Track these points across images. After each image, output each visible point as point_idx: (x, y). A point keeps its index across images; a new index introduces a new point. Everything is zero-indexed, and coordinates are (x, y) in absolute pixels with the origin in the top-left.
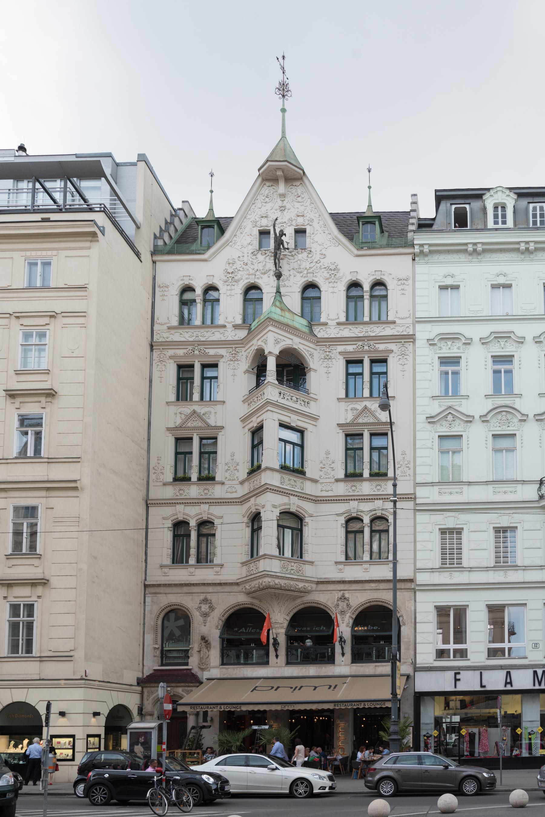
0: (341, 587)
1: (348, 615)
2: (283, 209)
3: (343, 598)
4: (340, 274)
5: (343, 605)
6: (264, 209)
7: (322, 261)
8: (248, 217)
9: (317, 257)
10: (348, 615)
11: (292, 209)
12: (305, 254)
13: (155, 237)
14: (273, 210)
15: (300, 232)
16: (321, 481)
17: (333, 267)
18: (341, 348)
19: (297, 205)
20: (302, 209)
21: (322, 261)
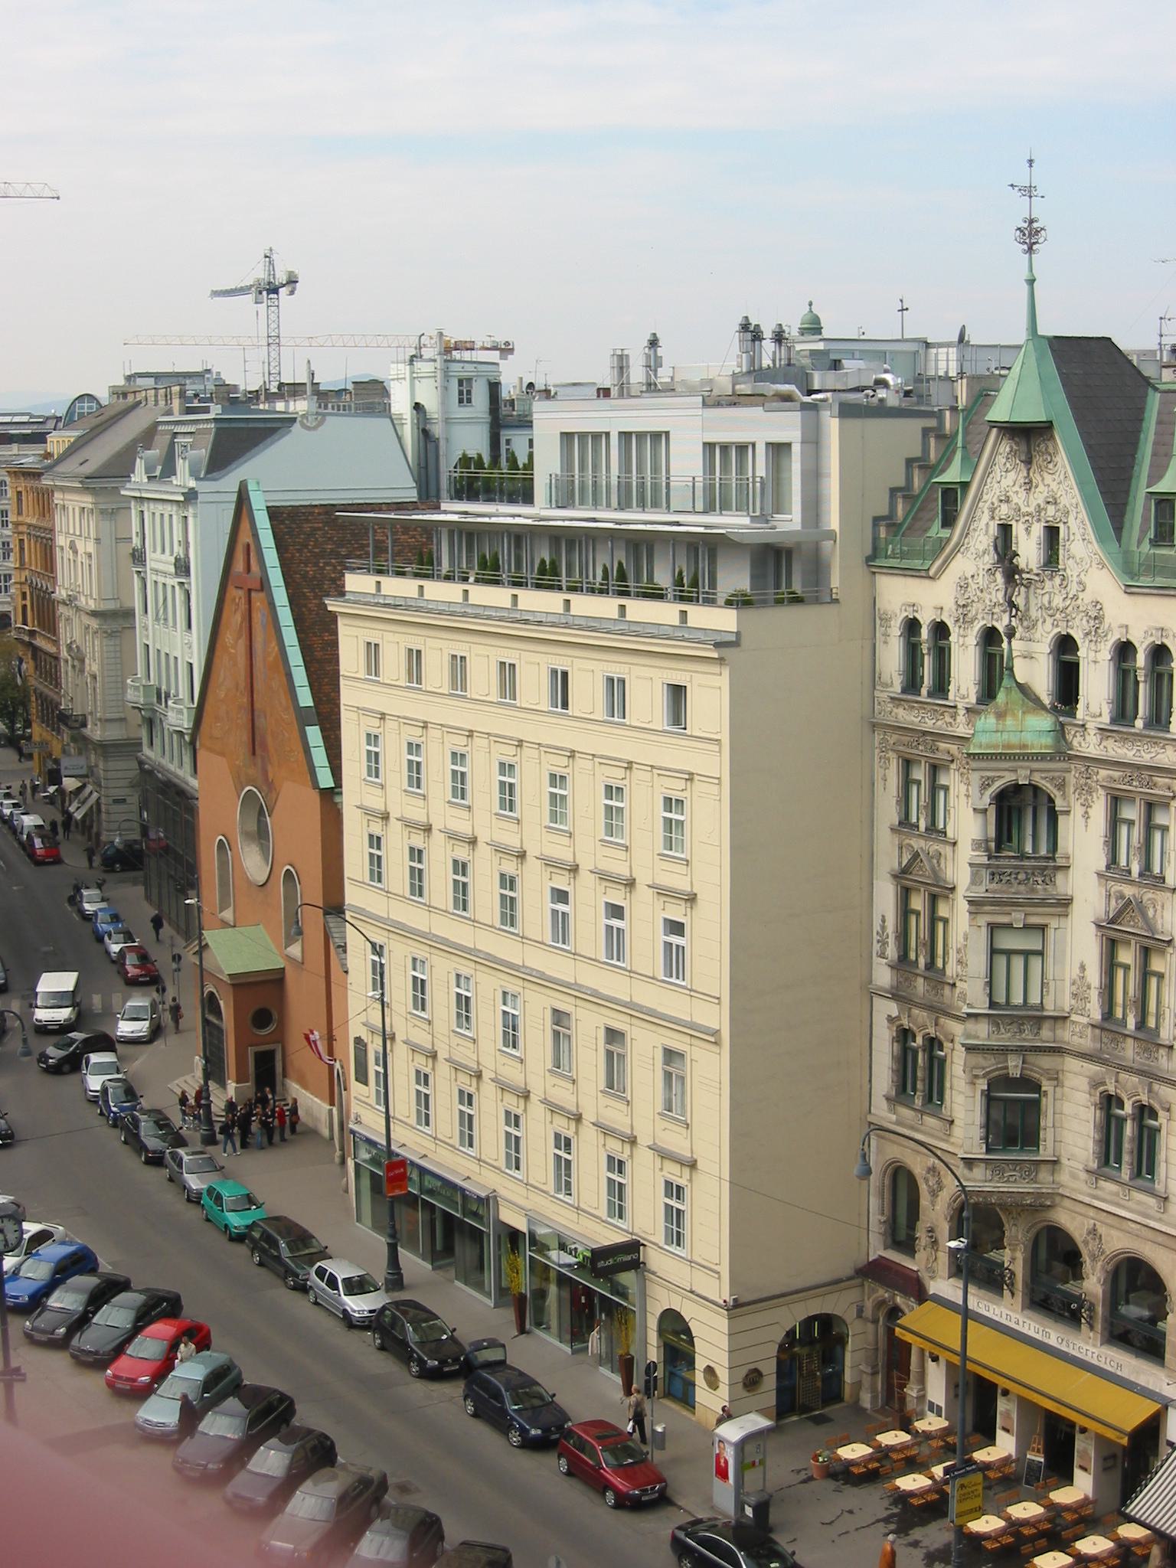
0: (1092, 1213)
1: (1100, 1263)
2: (1029, 485)
3: (1093, 1231)
4: (1107, 621)
5: (1093, 1245)
6: (1005, 483)
7: (1081, 595)
8: (985, 497)
9: (1073, 588)
10: (1100, 1263)
11: (1041, 488)
12: (1057, 580)
13: (877, 520)
14: (1016, 488)
15: (1052, 534)
16: (1074, 1017)
17: (1093, 614)
18: (1103, 773)
19: (1048, 479)
20: (1054, 486)
21: (1081, 595)
